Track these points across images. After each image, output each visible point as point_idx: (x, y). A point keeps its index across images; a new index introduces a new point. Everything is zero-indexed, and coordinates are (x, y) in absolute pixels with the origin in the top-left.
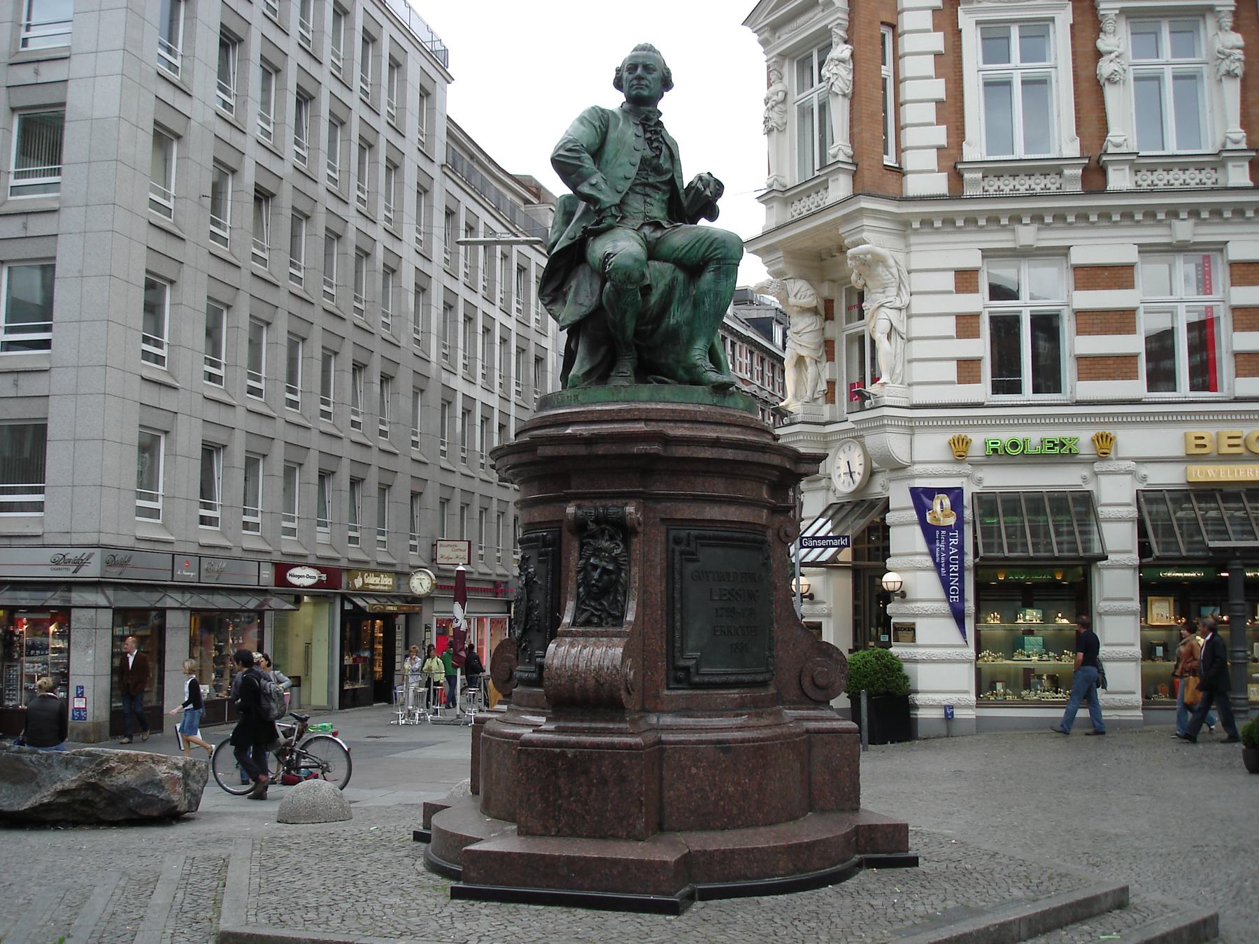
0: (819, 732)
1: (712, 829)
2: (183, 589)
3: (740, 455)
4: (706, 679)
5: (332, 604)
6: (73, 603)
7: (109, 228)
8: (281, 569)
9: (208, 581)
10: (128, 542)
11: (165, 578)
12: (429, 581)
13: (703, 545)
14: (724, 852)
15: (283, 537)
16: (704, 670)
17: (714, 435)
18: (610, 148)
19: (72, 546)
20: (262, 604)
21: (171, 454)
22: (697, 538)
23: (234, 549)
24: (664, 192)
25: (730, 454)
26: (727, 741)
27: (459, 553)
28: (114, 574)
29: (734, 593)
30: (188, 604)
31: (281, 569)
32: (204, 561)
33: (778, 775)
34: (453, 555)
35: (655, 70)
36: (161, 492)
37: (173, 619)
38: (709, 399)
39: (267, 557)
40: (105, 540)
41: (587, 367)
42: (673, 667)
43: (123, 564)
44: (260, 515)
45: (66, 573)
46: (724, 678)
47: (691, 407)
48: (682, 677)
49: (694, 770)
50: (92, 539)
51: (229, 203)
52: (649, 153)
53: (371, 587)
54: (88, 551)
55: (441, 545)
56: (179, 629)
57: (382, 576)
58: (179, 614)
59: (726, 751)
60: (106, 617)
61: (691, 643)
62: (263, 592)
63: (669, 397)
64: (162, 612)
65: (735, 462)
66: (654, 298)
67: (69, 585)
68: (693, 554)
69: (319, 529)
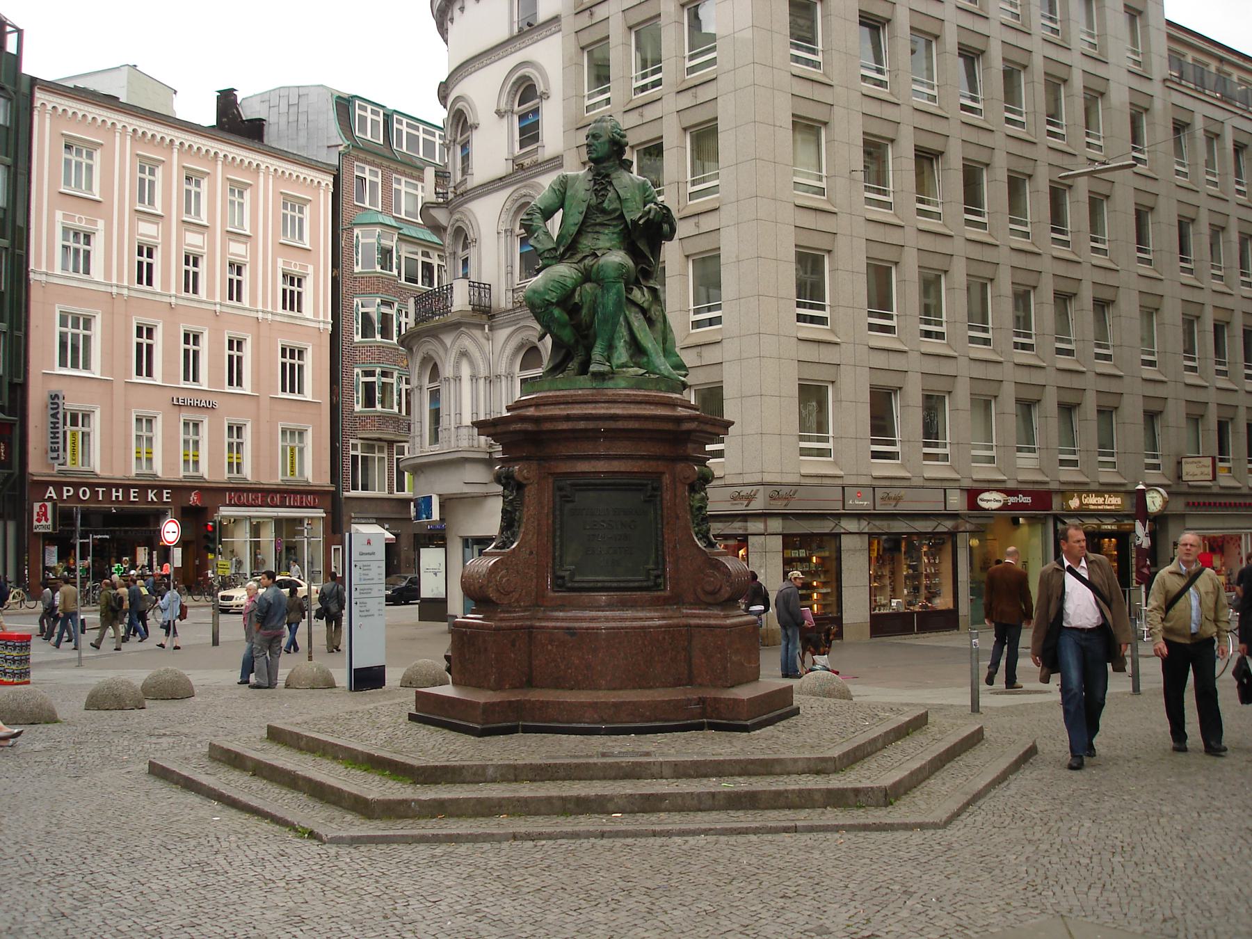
0: (698, 626)
1: (563, 688)
2: (859, 516)
3: (591, 425)
4: (576, 585)
5: (1044, 524)
6: (749, 531)
7: (754, 217)
8: (972, 495)
9: (881, 508)
10: (794, 479)
11: (837, 507)
12: (1161, 499)
14: (542, 702)
15: (973, 465)
16: (577, 578)
17: (565, 413)
18: (567, 203)
19: (744, 485)
20: (957, 527)
21: (837, 401)
22: (572, 485)
23: (914, 479)
24: (615, 226)
25: (582, 425)
26: (575, 628)
27: (1203, 469)
28: (778, 506)
30: (866, 530)
31: (972, 495)
32: (879, 493)
33: (622, 654)
34: (1198, 471)
35: (601, 136)
36: (831, 434)
37: (846, 542)
38: (589, 385)
39: (956, 484)
40: (768, 478)
41: (551, 365)
42: (556, 578)
43: (788, 498)
44: (948, 446)
45: (740, 508)
46: (591, 585)
47: (572, 392)
48: (559, 583)
49: (550, 647)
50: (757, 478)
51: (891, 173)
52: (594, 201)
53: (1092, 507)
54: (755, 488)
55: (1187, 463)
56: (855, 551)
57: (1107, 496)
58: (856, 538)
59: (573, 634)
60: (778, 542)
62: (954, 516)
63: (560, 386)
64: (838, 536)
65: (586, 430)
66: (584, 311)
67: (745, 517)
69: (1019, 454)
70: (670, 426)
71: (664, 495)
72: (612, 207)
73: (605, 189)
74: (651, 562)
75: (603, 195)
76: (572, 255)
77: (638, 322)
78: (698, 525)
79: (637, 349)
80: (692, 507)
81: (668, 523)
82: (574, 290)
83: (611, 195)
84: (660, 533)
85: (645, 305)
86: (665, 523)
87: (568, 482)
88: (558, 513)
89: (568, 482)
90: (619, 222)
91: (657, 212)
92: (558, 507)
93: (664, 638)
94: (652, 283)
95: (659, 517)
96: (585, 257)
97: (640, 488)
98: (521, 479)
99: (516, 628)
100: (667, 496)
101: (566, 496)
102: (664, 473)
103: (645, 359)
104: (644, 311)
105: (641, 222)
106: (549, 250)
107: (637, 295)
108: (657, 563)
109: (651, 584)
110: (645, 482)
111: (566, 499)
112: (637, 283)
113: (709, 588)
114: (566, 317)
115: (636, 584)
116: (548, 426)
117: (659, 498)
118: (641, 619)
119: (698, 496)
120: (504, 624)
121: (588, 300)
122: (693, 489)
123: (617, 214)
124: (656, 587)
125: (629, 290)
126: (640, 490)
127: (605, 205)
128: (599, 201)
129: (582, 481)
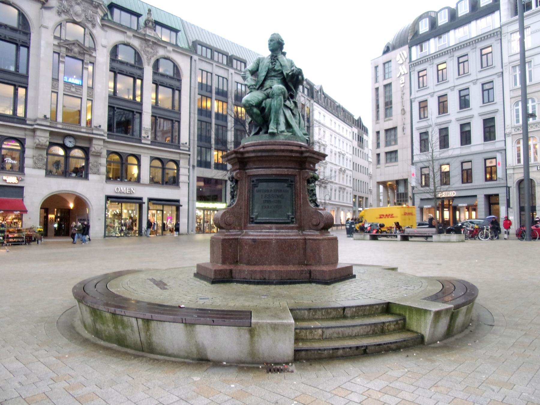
0: (310, 239)
13: (259, 182)
22: (257, 180)
24: (280, 77)
46: (264, 221)
52: (271, 66)
61: (256, 210)
65: (262, 156)
70: (298, 155)
72: (278, 69)
73: (275, 61)
75: (274, 64)
76: (262, 88)
77: (288, 113)
78: (311, 197)
79: (288, 125)
80: (308, 190)
82: (262, 101)
83: (278, 64)
84: (294, 200)
85: (292, 108)
88: (251, 192)
90: (281, 75)
91: (296, 71)
92: (251, 188)
93: (294, 244)
94: (294, 100)
95: (294, 194)
96: (267, 89)
97: (285, 181)
98: (235, 178)
99: (232, 239)
100: (298, 185)
101: (254, 185)
103: (291, 130)
104: (291, 110)
105: (290, 74)
106: (252, 85)
107: (288, 103)
108: (293, 213)
109: (289, 221)
111: (255, 186)
112: (288, 99)
113: (315, 223)
114: (258, 112)
115: (283, 221)
116: (247, 155)
117: (294, 186)
118: (284, 236)
119: (311, 185)
120: (226, 237)
121: (268, 106)
122: (309, 182)
123: (281, 71)
124: (292, 222)
125: (285, 101)
126: (286, 182)
127: (276, 68)
128: (273, 66)
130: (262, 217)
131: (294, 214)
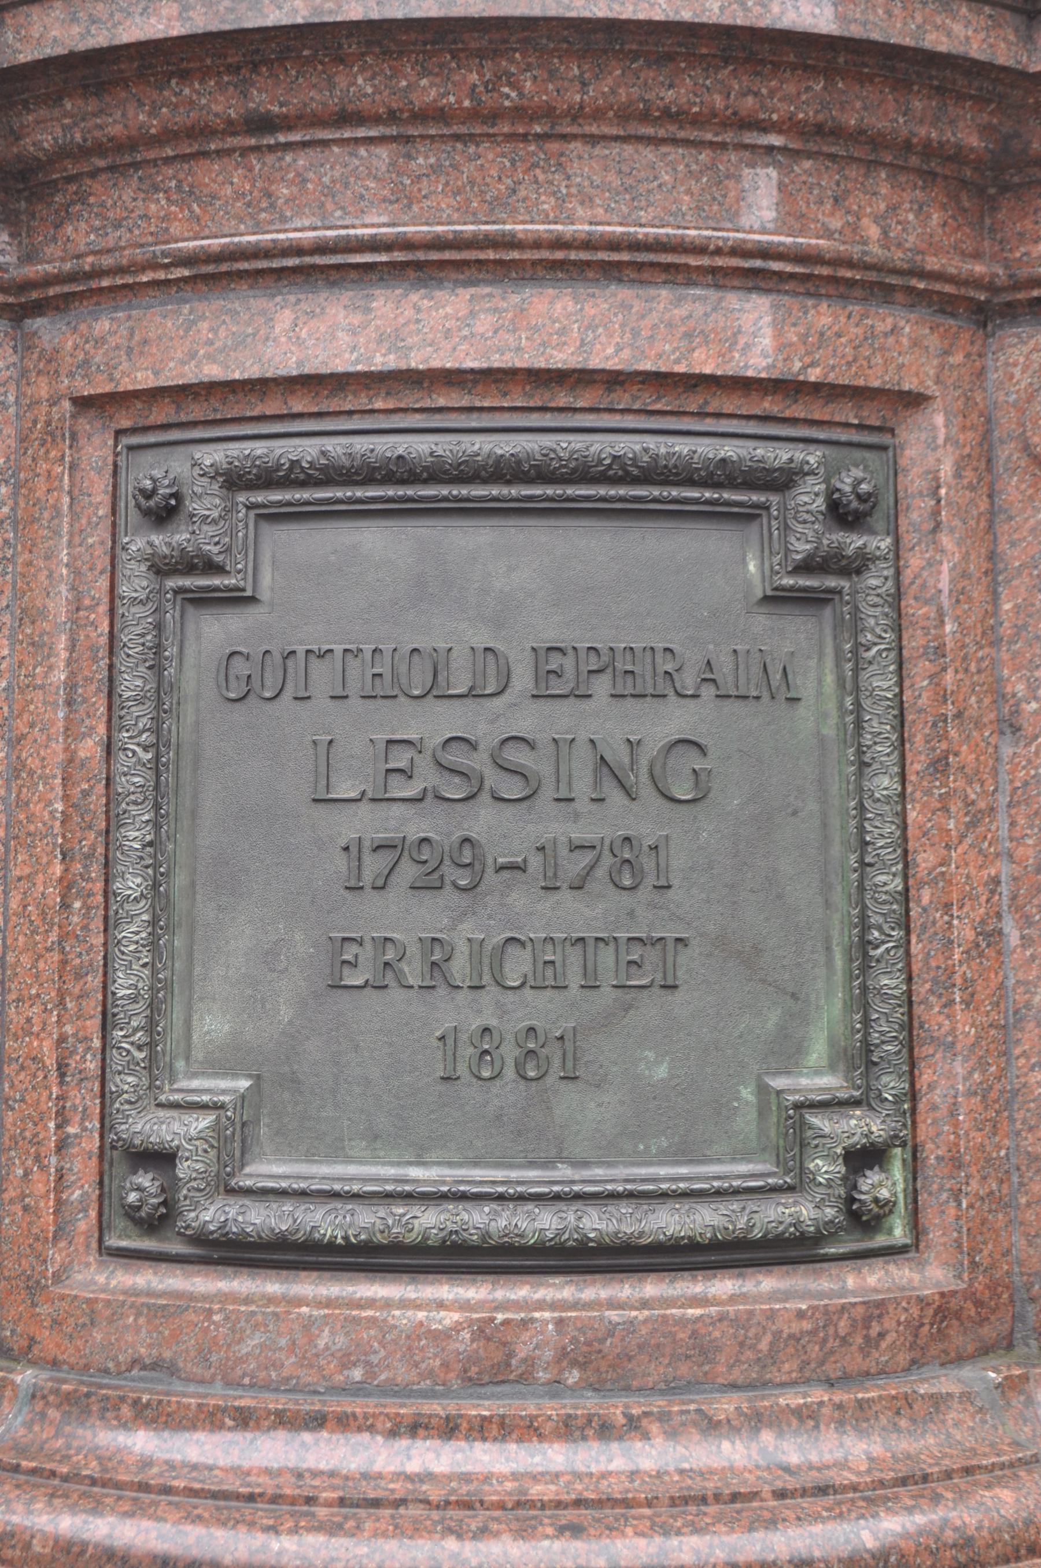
29: (479, 762)
68: (212, 567)
71: (914, 562)
74: (818, 1051)
81: (939, 766)
86: (916, 766)
87: (213, 456)
89: (213, 456)
102: (915, 400)
110: (780, 455)
117: (876, 579)
126: (748, 516)
129: (307, 451)
130: (338, 1153)
131: (891, 1084)
